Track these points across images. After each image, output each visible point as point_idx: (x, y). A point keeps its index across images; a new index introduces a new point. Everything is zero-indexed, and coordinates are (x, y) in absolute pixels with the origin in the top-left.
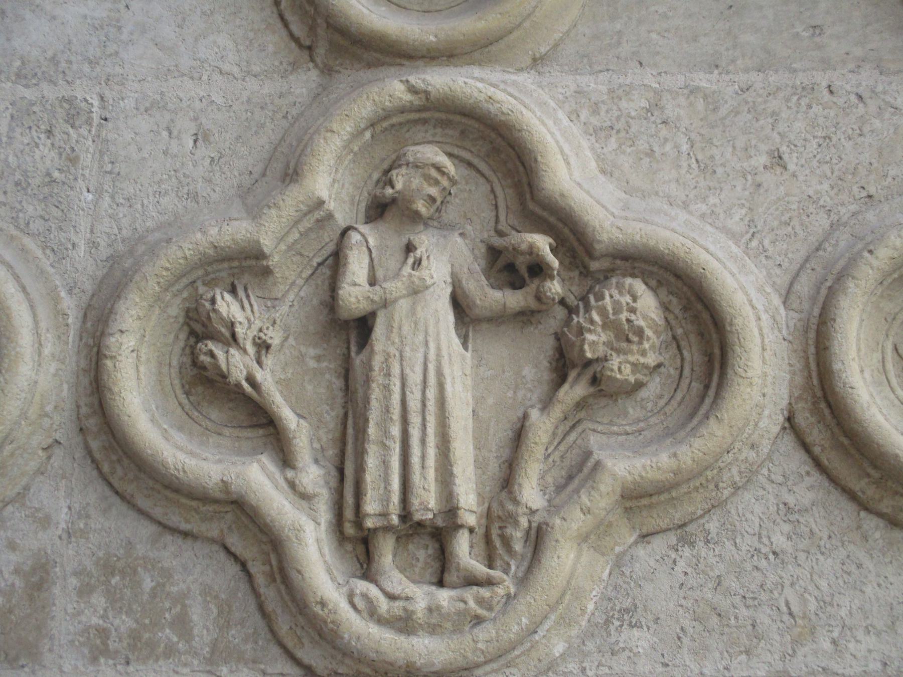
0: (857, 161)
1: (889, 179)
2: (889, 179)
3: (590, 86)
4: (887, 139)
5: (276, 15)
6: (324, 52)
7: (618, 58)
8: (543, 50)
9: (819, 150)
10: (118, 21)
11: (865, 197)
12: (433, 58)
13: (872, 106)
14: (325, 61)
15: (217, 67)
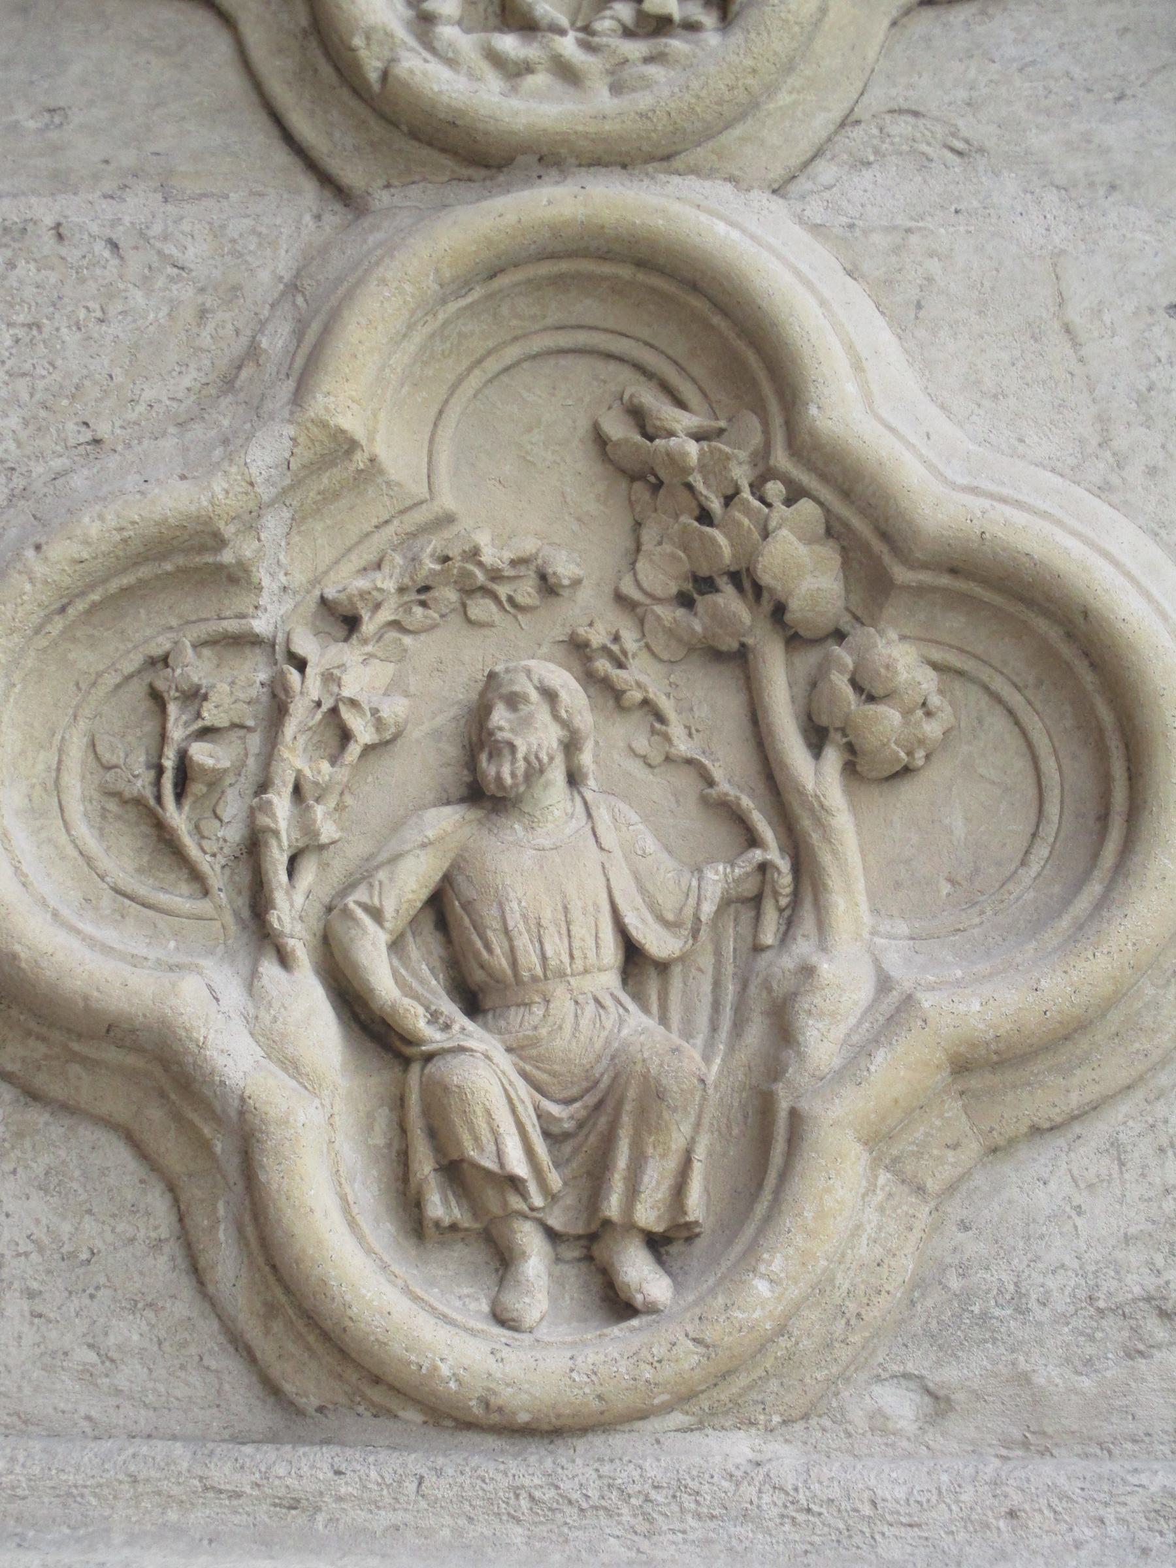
0: (85, 372)
1: (141, 408)
2: (141, 408)
4: (152, 328)
9: (14, 351)
11: (88, 443)
13: (136, 263)
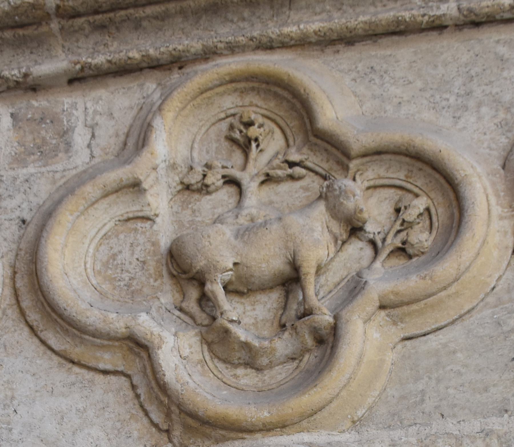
3: (401, 439)
5: (137, 406)
6: (179, 434)
7: (423, 413)
8: (360, 413)
10: (9, 423)
12: (269, 430)
14: (181, 441)
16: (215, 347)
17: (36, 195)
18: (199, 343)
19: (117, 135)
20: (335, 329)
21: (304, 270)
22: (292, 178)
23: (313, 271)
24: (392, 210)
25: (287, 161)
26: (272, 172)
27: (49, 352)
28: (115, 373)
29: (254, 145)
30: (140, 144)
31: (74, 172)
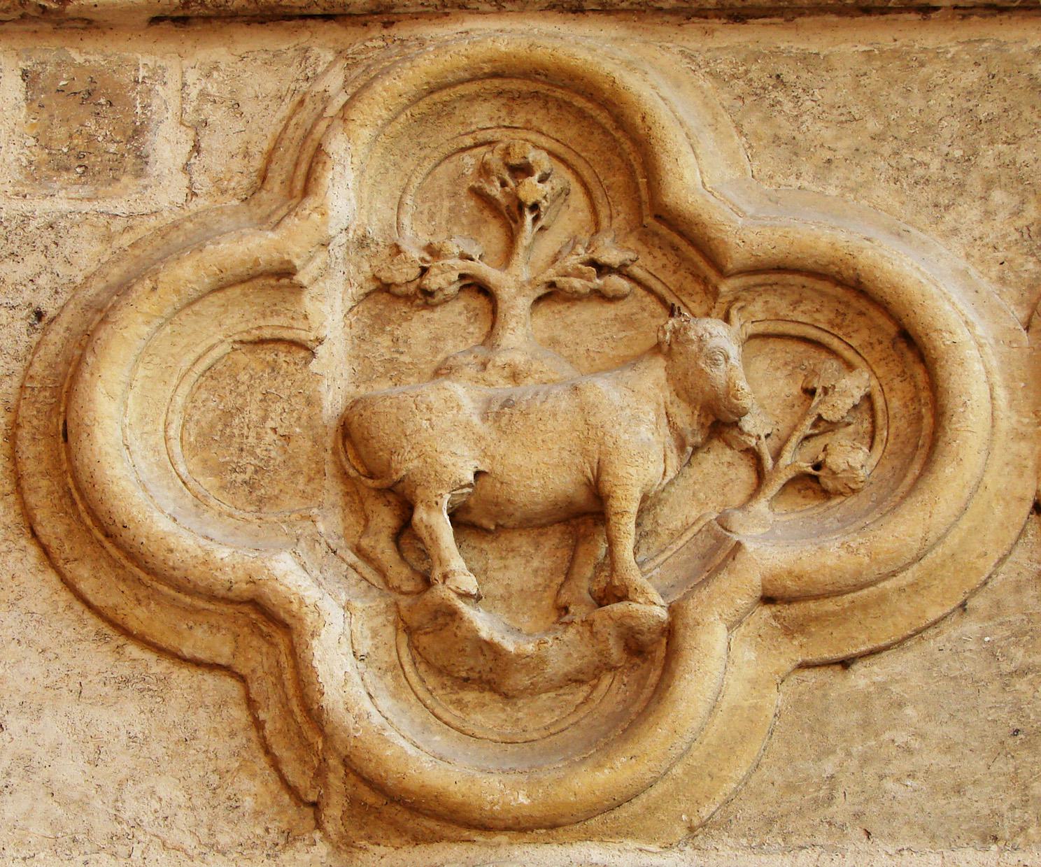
5: (255, 746)
6: (340, 814)
7: (830, 824)
8: (705, 814)
14: (342, 829)
15: (157, 836)
16: (424, 640)
17: (68, 262)
18: (391, 629)
19: (246, 155)
20: (669, 632)
21: (616, 505)
22: (601, 296)
23: (634, 508)
24: (796, 390)
25: (593, 263)
26: (562, 282)
27: (78, 606)
28: (213, 667)
29: (529, 217)
30: (299, 184)
31: (153, 222)
